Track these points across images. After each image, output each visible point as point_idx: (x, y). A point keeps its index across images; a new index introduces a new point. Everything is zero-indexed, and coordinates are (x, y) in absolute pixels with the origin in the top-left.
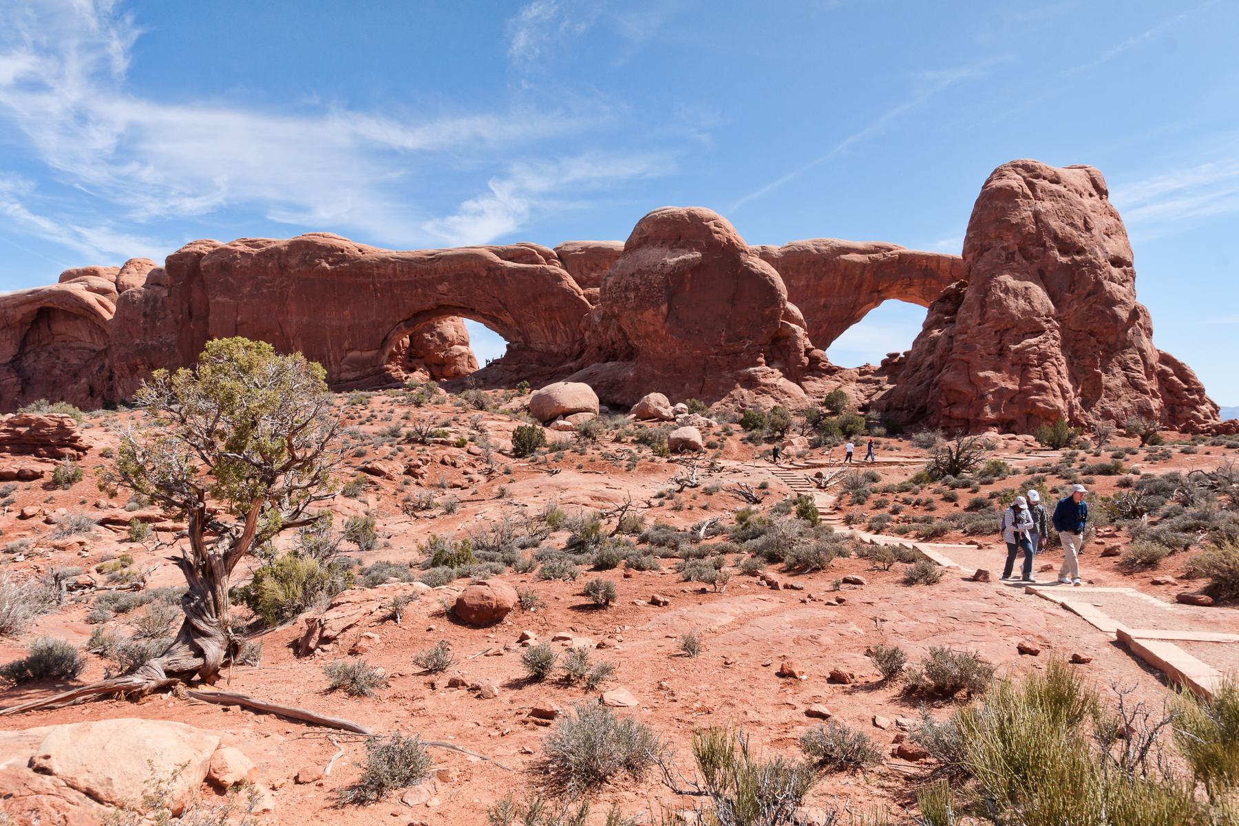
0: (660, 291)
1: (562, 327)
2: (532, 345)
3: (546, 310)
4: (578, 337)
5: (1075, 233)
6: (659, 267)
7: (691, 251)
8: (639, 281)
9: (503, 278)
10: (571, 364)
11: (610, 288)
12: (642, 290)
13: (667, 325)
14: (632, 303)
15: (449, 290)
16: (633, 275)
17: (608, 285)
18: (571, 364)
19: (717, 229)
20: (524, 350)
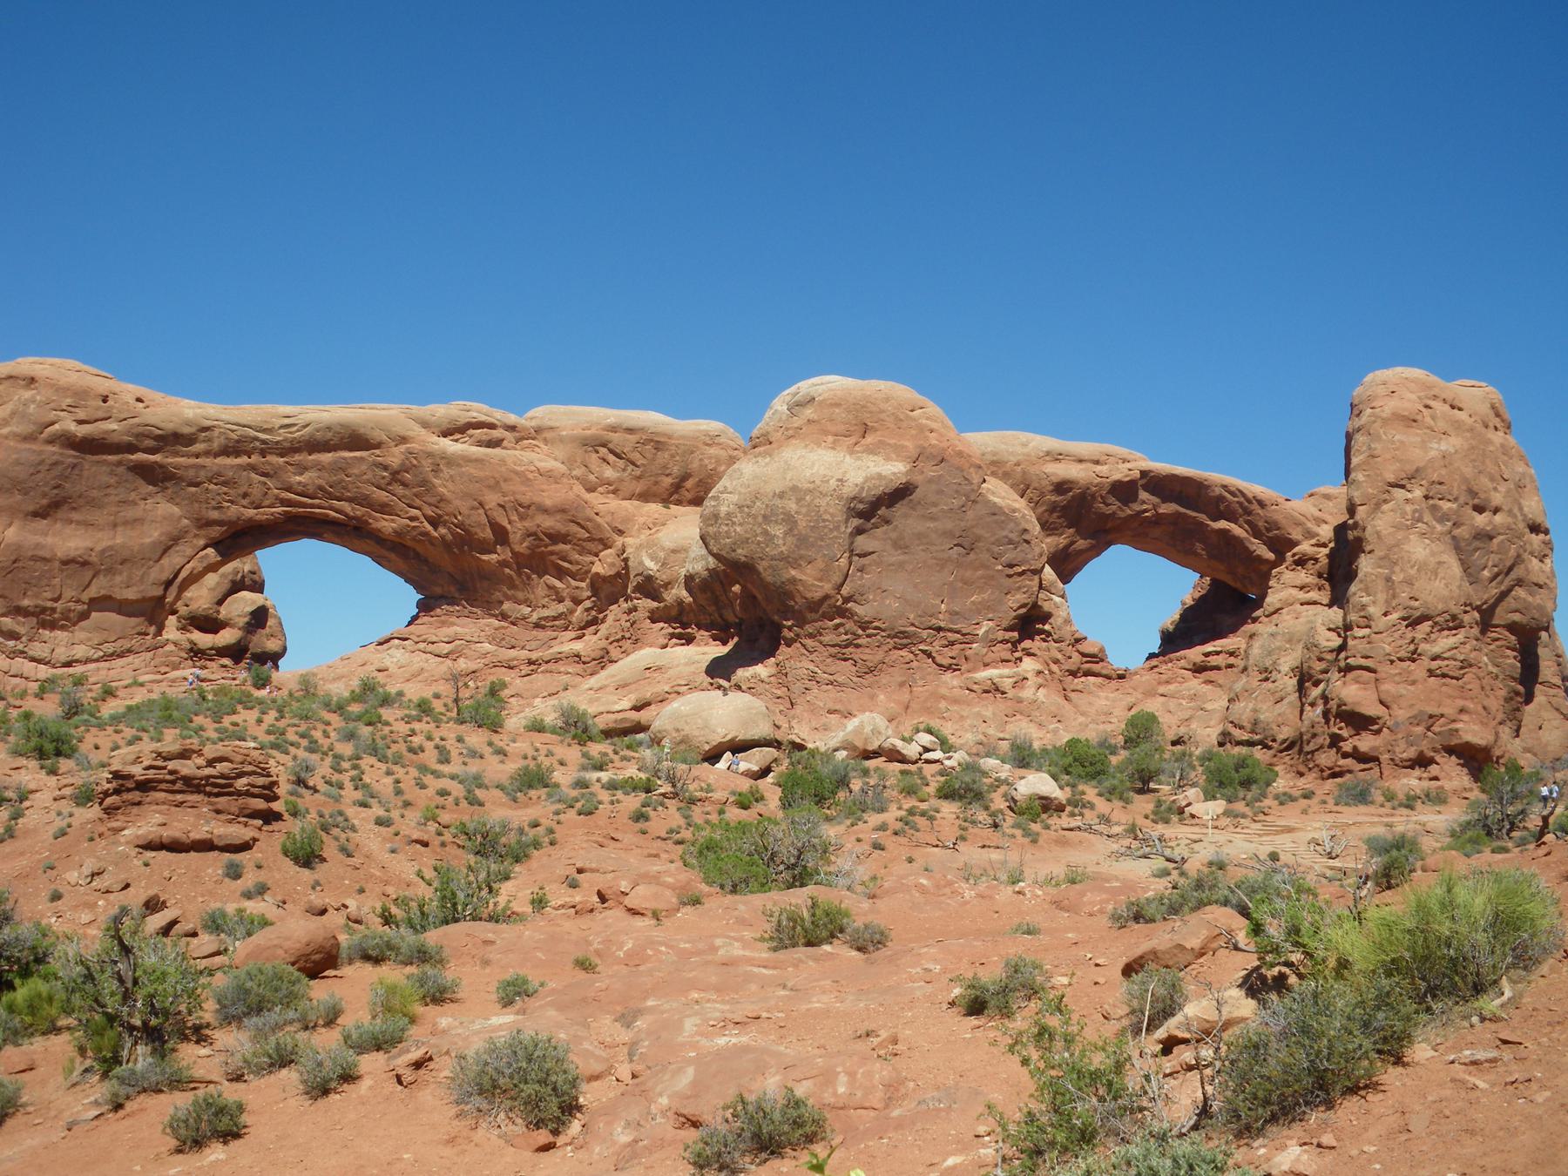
5: (1490, 485)
6: (833, 483)
7: (888, 459)
11: (728, 514)
16: (782, 495)
19: (934, 425)
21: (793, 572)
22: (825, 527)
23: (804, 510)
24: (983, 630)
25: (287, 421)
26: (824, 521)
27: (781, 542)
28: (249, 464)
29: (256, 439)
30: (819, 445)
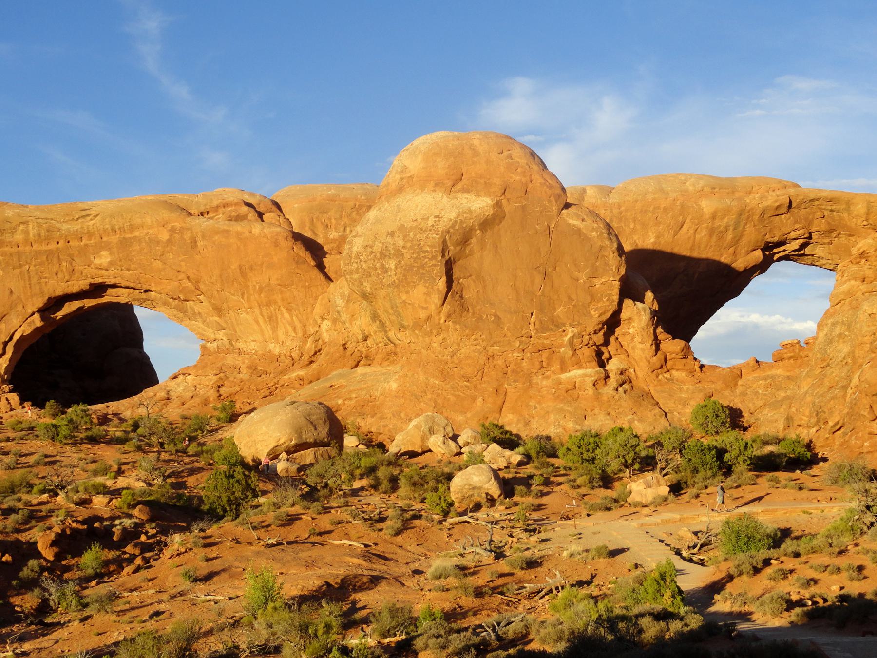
0: (434, 258)
1: (286, 315)
2: (240, 345)
3: (261, 290)
4: (312, 330)
6: (431, 221)
8: (401, 243)
9: (194, 242)
10: (301, 373)
11: (358, 254)
12: (407, 255)
13: (446, 308)
14: (392, 276)
15: (111, 263)
16: (392, 234)
17: (355, 249)
18: (301, 373)
20: (227, 352)
21: (404, 297)
22: (425, 257)
23: (409, 245)
24: (570, 335)
25: (84, 213)
26: (425, 252)
27: (393, 273)
28: (57, 249)
29: (59, 230)
30: (423, 190)
